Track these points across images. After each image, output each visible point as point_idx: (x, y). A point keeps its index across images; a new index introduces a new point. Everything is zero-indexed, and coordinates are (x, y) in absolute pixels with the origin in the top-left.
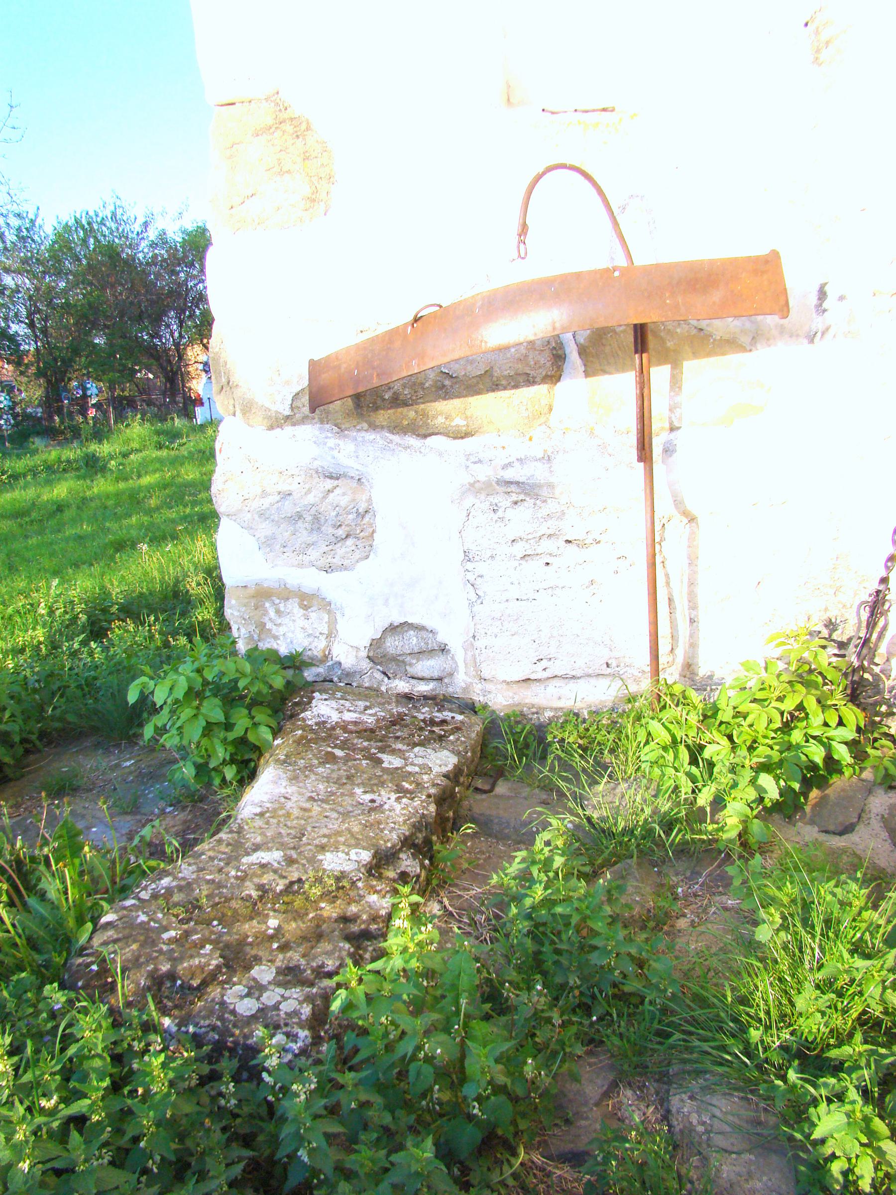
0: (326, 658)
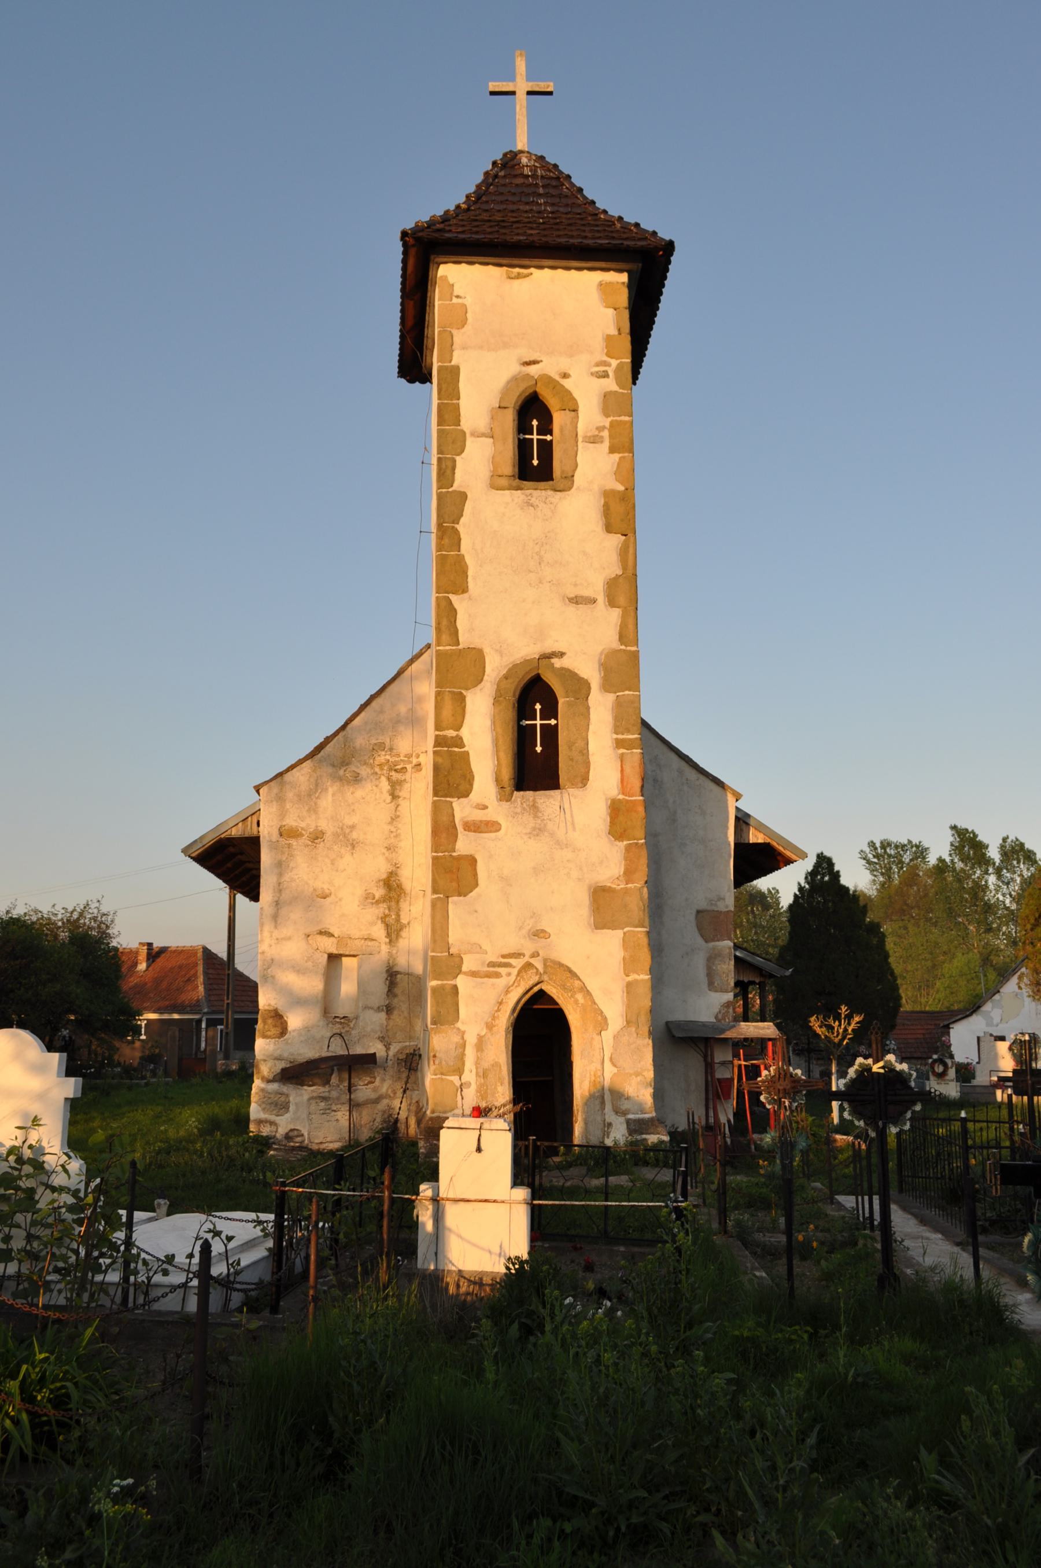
0: (275, 1136)
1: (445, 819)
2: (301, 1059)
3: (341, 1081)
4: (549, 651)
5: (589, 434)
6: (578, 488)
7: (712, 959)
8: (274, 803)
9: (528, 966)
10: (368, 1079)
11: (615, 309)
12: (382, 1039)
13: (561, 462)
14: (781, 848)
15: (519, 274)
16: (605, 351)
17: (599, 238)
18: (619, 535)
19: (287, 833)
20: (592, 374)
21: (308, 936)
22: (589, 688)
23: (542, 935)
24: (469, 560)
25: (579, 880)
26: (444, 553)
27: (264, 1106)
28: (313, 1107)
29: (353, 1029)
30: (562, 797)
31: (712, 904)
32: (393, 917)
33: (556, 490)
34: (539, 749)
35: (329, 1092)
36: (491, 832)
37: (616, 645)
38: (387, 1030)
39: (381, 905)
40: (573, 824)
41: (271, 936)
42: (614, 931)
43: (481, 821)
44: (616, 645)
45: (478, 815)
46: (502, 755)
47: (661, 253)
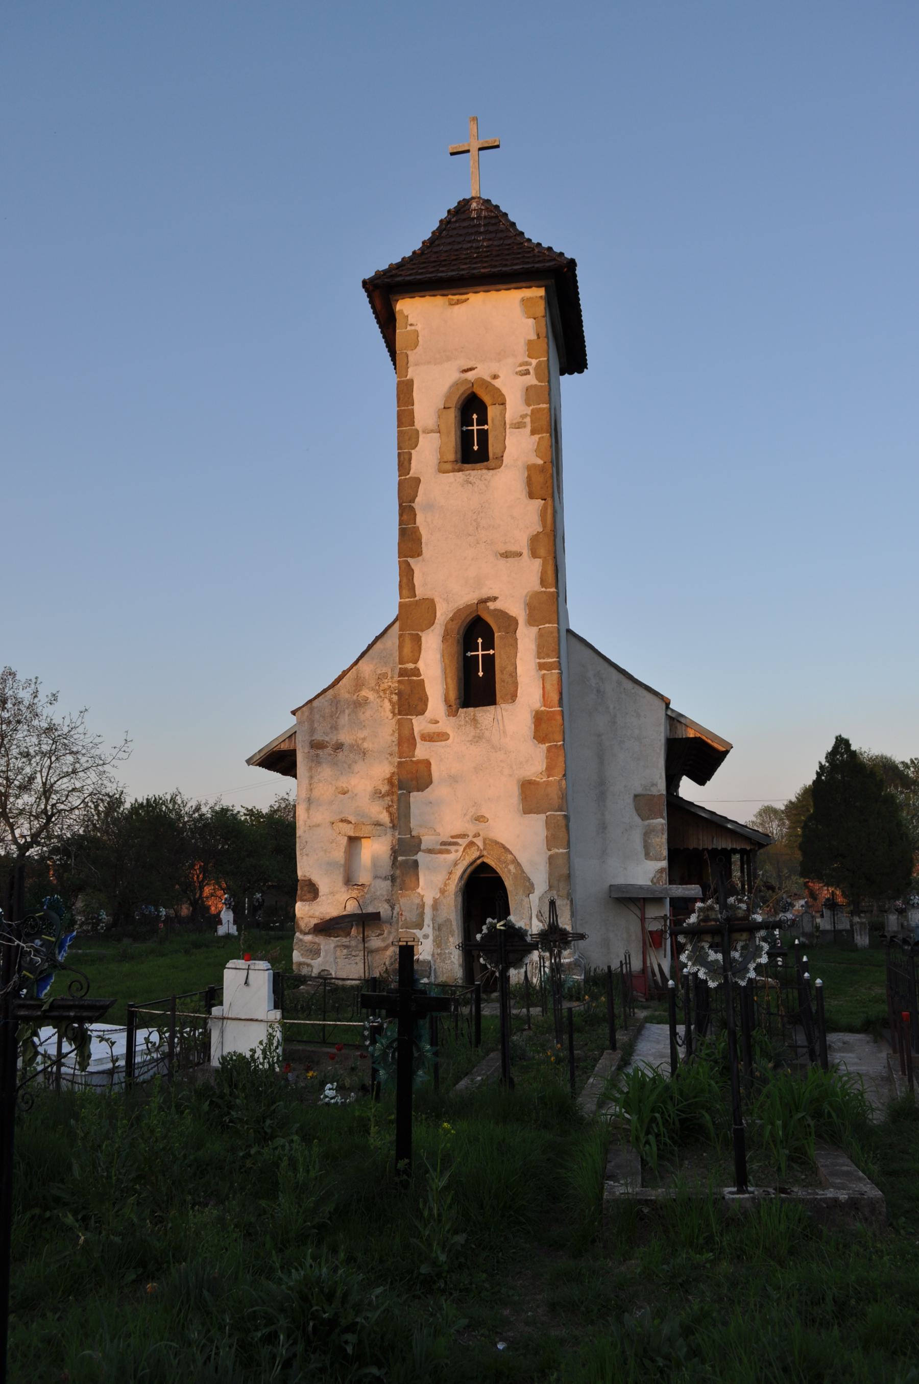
0: (311, 975)
1: (406, 732)
2: (328, 917)
3: (358, 933)
4: (485, 596)
5: (515, 422)
6: (506, 466)
7: (647, 834)
8: (306, 723)
9: (471, 844)
10: (379, 932)
11: (535, 319)
12: (388, 901)
13: (493, 446)
14: (709, 741)
15: (458, 300)
16: (527, 353)
17: (516, 264)
18: (540, 500)
19: (317, 746)
20: (517, 373)
21: (333, 823)
22: (517, 624)
23: (482, 820)
24: (423, 531)
25: (510, 775)
26: (403, 526)
27: (302, 952)
28: (338, 953)
29: (366, 893)
30: (496, 711)
31: (646, 790)
32: (395, 807)
33: (489, 469)
34: (481, 674)
35: (349, 941)
36: (441, 741)
37: (537, 587)
38: (392, 895)
39: (386, 798)
40: (504, 732)
41: (305, 824)
42: (539, 815)
43: (434, 733)
44: (537, 587)
45: (432, 728)
46: (449, 680)
47: (566, 270)
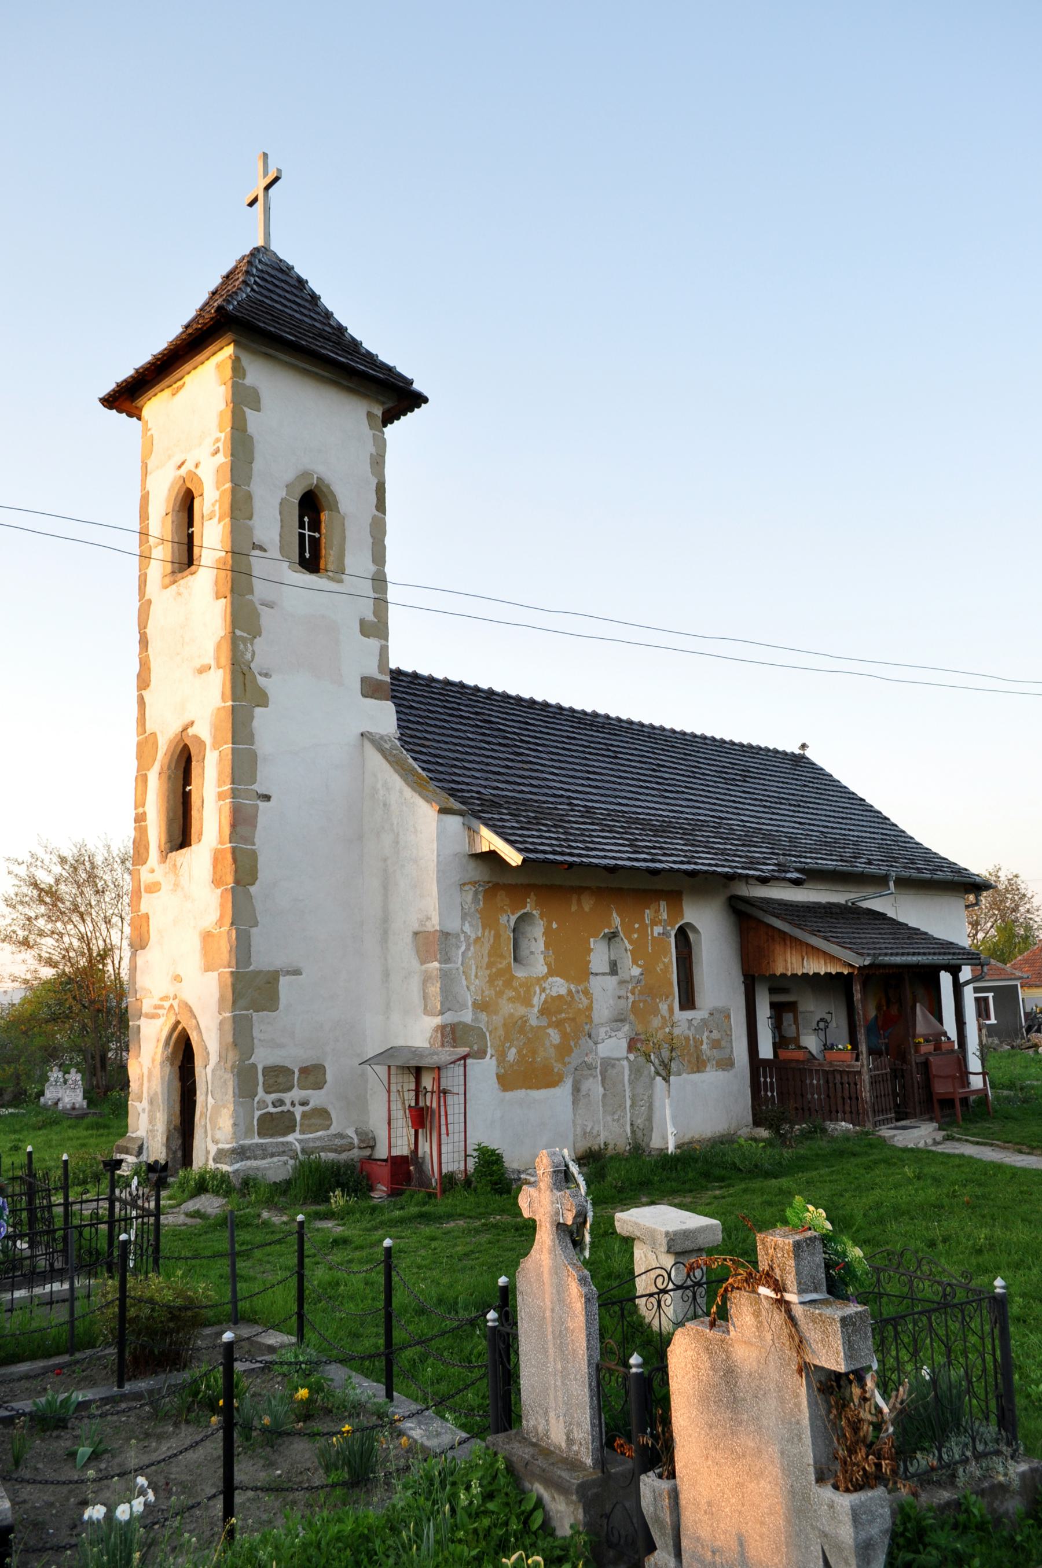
7: (426, 980)
